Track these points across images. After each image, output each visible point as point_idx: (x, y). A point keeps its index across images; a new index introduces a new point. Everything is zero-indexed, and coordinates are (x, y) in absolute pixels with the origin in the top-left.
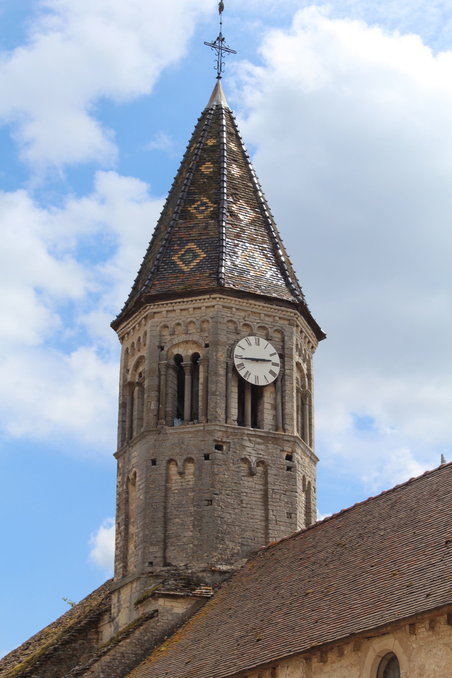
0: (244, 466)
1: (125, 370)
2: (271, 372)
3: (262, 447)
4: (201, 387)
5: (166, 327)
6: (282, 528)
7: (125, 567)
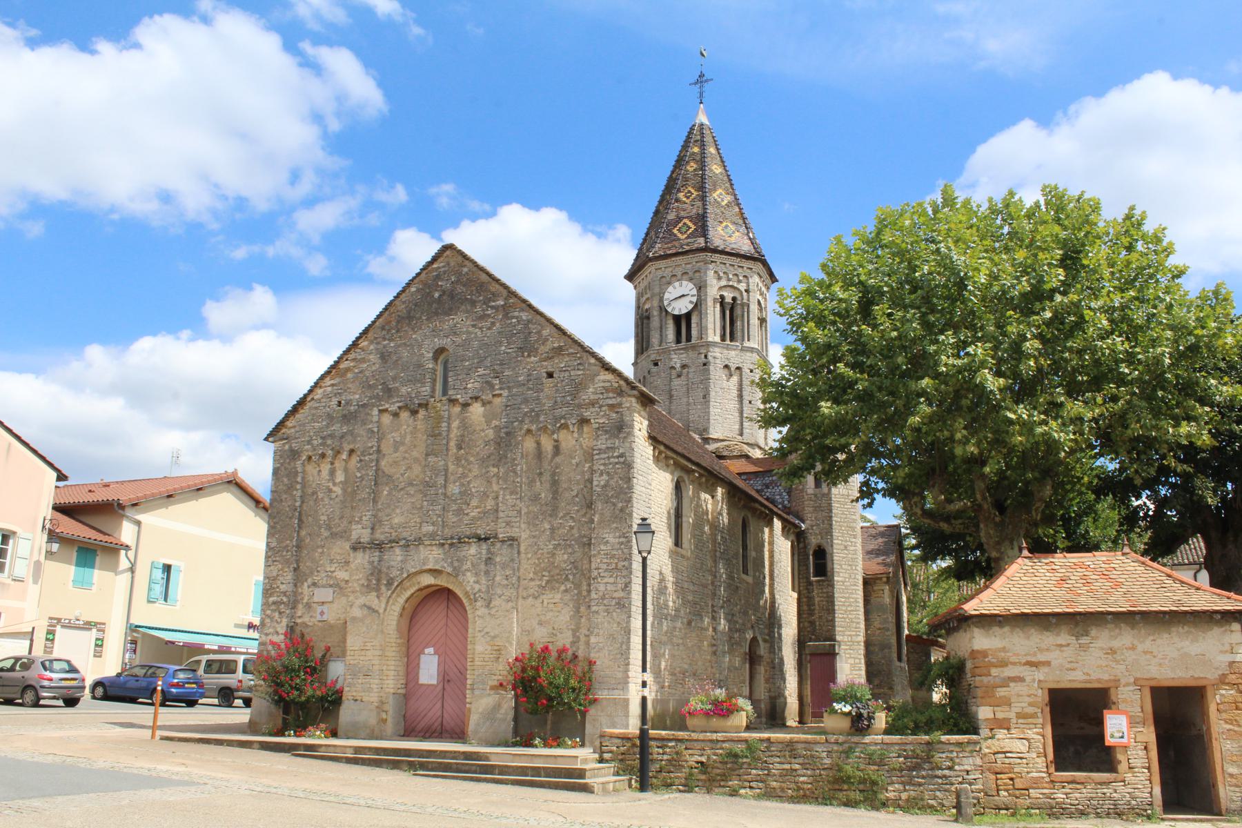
2: (691, 302)
3: (684, 355)
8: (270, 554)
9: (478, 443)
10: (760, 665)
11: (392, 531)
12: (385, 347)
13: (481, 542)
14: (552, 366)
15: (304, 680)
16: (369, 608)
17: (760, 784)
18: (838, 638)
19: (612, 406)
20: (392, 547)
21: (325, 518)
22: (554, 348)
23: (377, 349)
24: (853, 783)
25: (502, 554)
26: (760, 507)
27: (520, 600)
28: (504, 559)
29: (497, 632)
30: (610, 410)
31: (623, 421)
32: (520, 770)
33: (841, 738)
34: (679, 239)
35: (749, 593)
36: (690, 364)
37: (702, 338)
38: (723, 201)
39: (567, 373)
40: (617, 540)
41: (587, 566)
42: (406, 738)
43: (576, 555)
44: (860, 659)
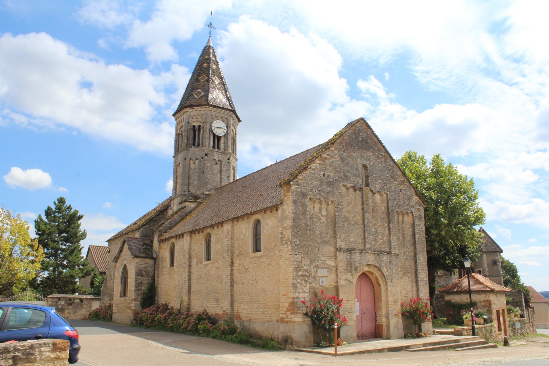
0: (214, 162)
1: (177, 129)
2: (224, 132)
3: (220, 155)
4: (201, 136)
5: (190, 116)
7: (176, 192)
11: (350, 244)
16: (349, 280)
22: (401, 181)
43: (411, 263)
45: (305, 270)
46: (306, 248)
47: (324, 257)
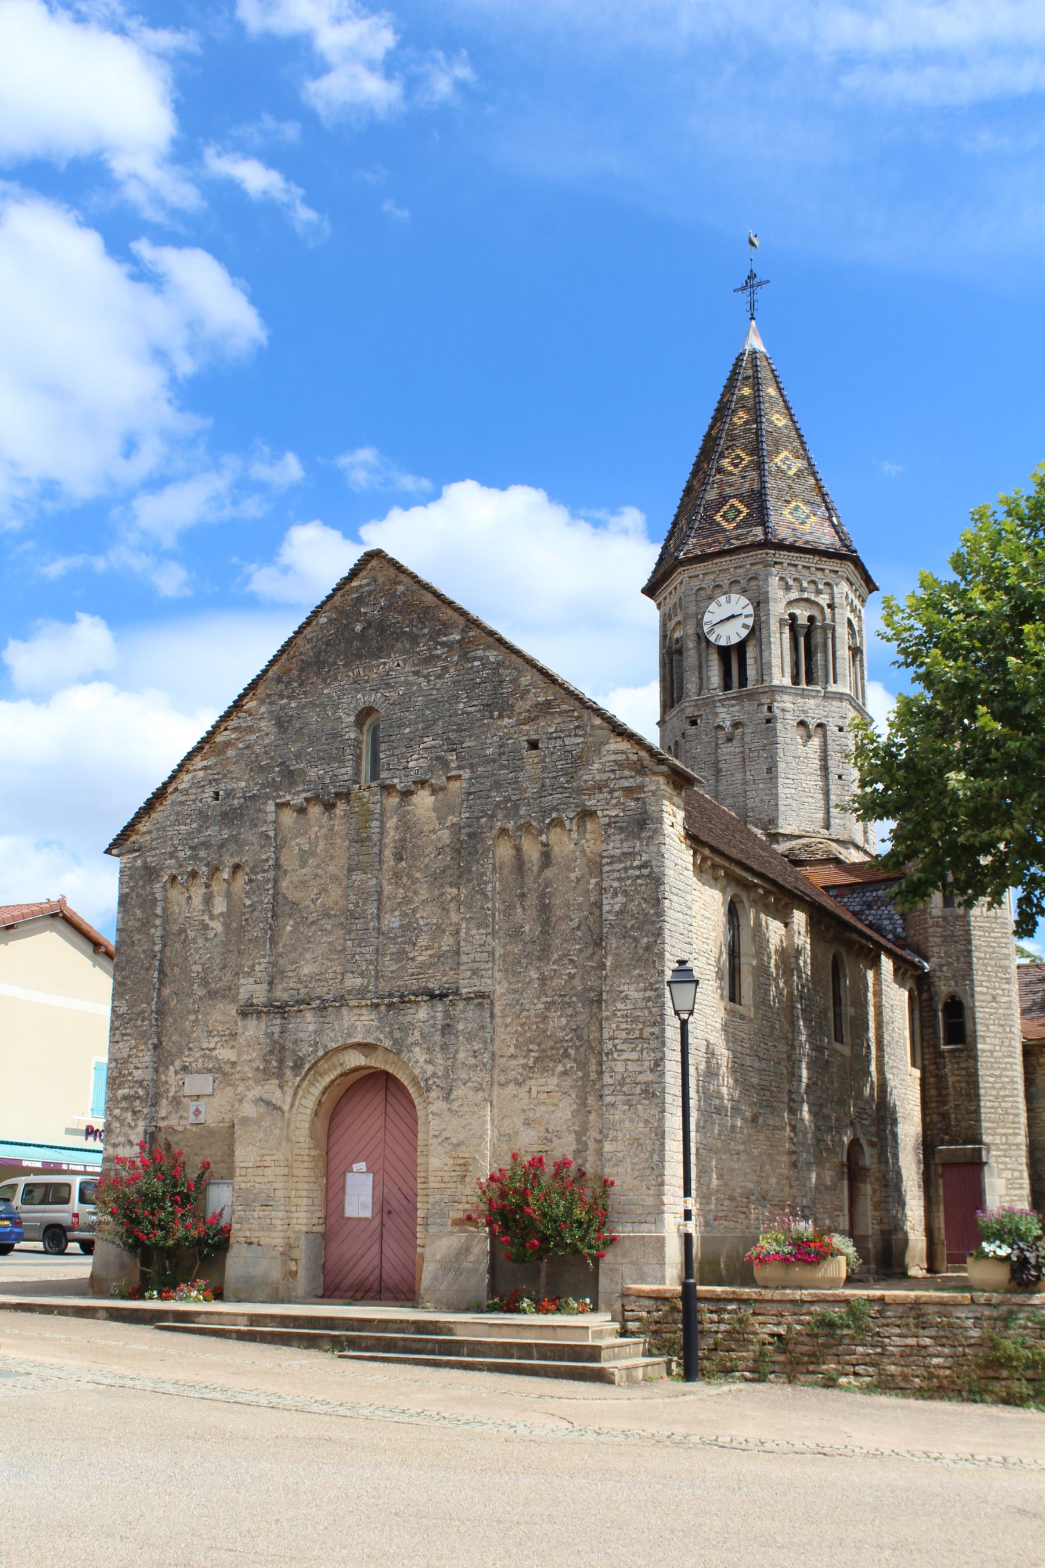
2: (745, 626)
3: (737, 708)
6: (761, 786)
8: (117, 1024)
9: (427, 851)
10: (865, 1182)
11: (299, 986)
12: (282, 708)
13: (435, 1001)
14: (537, 730)
15: (172, 1213)
16: (268, 1103)
17: (870, 1369)
18: (986, 1139)
19: (628, 791)
20: (301, 1011)
21: (199, 968)
22: (538, 704)
23: (271, 712)
24: (1016, 1368)
25: (467, 1019)
26: (859, 939)
27: (496, 1088)
28: (470, 1026)
29: (461, 1138)
30: (626, 796)
31: (646, 812)
32: (500, 1348)
33: (996, 1298)
34: (724, 530)
35: (845, 1072)
36: (746, 721)
37: (763, 681)
38: (789, 468)
39: (559, 742)
40: (641, 995)
41: (597, 1035)
42: (330, 1300)
43: (579, 1018)
44: (1021, 1171)
45: (136, 1082)
46: (142, 1021)
47: (211, 1039)
